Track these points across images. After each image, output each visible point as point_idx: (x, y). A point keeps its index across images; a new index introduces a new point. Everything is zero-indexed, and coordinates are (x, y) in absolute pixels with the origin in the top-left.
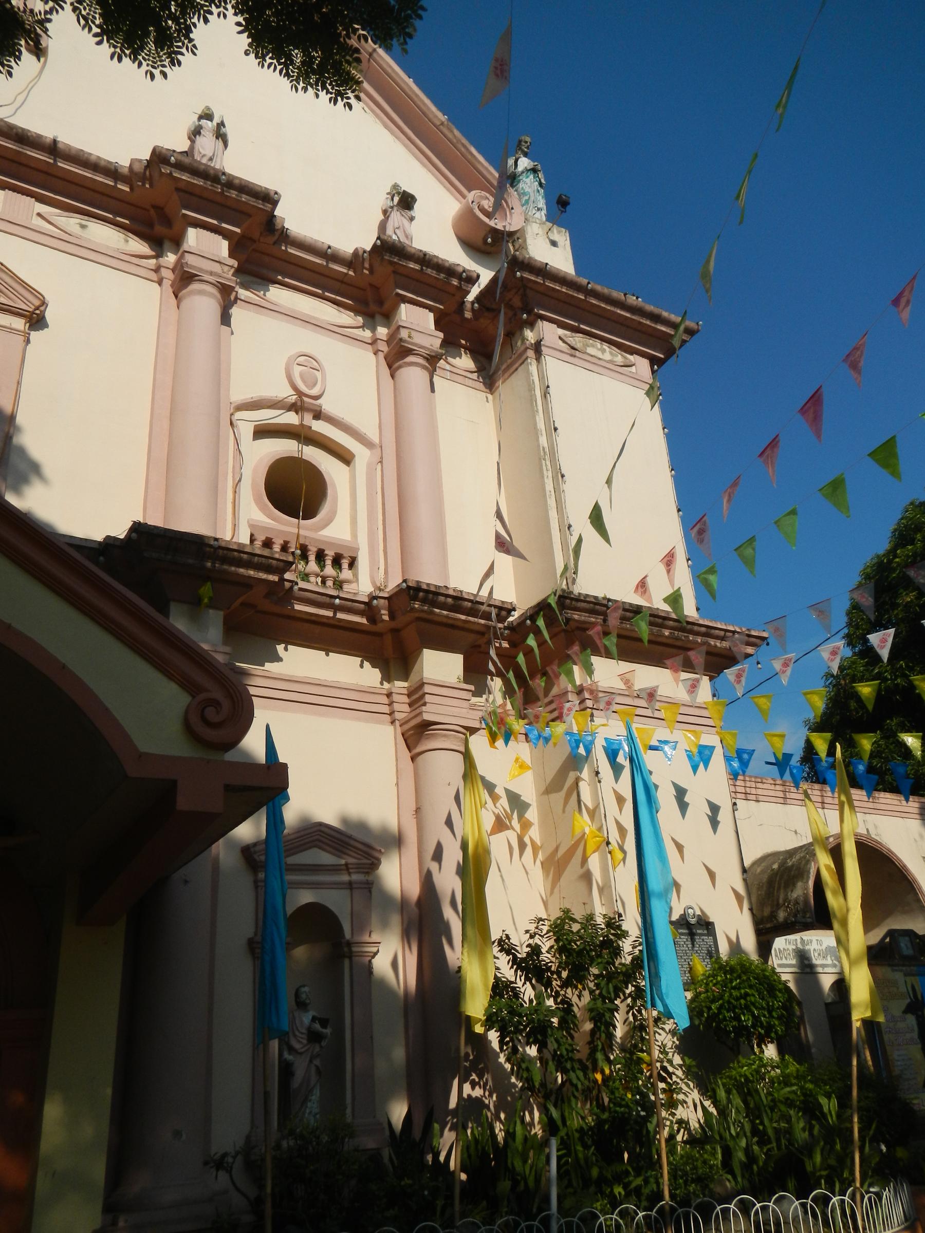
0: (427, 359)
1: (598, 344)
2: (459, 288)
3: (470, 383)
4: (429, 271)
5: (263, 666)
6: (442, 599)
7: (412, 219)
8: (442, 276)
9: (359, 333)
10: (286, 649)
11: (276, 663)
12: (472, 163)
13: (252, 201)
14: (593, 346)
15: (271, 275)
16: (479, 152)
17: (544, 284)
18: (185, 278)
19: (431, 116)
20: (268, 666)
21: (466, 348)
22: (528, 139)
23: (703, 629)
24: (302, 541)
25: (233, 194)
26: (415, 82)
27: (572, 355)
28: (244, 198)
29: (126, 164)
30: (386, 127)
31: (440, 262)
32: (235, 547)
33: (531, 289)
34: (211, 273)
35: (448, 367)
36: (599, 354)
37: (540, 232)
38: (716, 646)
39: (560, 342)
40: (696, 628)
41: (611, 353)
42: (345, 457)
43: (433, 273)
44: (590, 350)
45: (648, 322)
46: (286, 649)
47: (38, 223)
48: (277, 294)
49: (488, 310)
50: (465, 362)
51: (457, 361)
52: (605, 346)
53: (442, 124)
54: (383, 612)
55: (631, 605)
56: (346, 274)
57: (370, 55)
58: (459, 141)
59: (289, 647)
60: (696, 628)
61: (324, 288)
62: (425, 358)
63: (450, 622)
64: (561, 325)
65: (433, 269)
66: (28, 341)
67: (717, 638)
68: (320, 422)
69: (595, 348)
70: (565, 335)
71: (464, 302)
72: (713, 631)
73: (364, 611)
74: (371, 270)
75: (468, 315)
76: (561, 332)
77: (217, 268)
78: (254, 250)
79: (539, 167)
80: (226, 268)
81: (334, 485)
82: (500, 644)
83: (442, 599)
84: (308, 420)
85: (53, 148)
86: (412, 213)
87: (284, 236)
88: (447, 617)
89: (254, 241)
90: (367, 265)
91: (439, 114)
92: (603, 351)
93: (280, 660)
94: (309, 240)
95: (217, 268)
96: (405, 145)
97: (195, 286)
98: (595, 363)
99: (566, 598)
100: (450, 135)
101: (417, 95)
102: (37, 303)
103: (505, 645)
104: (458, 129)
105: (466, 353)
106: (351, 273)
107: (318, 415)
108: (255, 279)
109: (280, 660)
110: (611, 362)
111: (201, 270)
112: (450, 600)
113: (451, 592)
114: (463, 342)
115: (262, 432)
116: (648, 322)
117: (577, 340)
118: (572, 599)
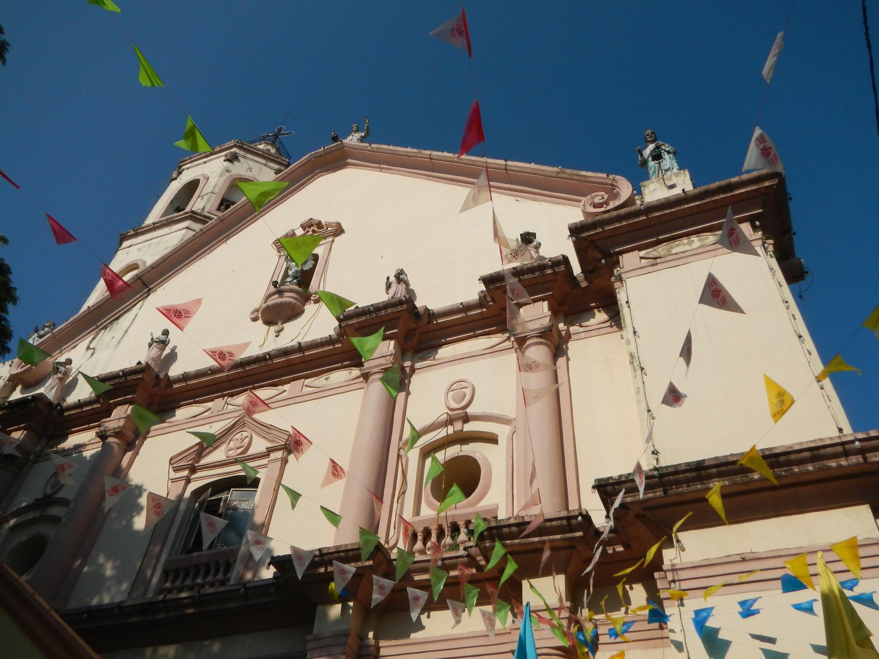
0: (541, 337)
1: (685, 240)
2: (554, 273)
3: (605, 331)
4: (526, 277)
5: (408, 636)
6: (506, 530)
7: (537, 247)
8: (537, 274)
9: (508, 344)
10: (428, 617)
11: (420, 632)
12: (585, 180)
13: (394, 310)
14: (678, 245)
15: (436, 342)
16: (587, 171)
17: (604, 230)
18: (366, 376)
19: (550, 174)
20: (414, 636)
21: (597, 307)
22: (649, 132)
23: (806, 454)
24: (450, 520)
25: (383, 312)
26: (536, 163)
27: (653, 265)
28: (389, 311)
29: (333, 333)
30: (533, 200)
31: (530, 266)
32: (333, 550)
33: (598, 240)
34: (376, 366)
35: (582, 329)
36: (687, 248)
37: (658, 185)
38: (840, 467)
39: (643, 261)
40: (793, 457)
41: (700, 240)
42: (492, 439)
43: (530, 276)
44: (674, 251)
45: (722, 196)
46: (428, 617)
47: (306, 390)
48: (444, 352)
49: (591, 272)
50: (601, 316)
51: (592, 321)
52: (694, 238)
53: (558, 173)
54: (478, 558)
55: (688, 464)
56: (482, 313)
57: (506, 169)
58: (571, 175)
59: (432, 613)
60: (793, 457)
61: (474, 329)
62: (537, 337)
63: (531, 547)
64: (640, 248)
65: (527, 273)
66: (286, 462)
67: (836, 456)
68: (471, 423)
69: (681, 246)
70: (647, 253)
71: (575, 278)
72: (822, 451)
73: (469, 562)
74: (493, 300)
75: (584, 284)
76: (642, 253)
77: (383, 361)
78: (421, 334)
79: (660, 143)
80: (388, 358)
81: (488, 465)
82: (614, 549)
83: (506, 530)
84: (458, 426)
85: (300, 348)
86: (534, 243)
87: (430, 315)
88: (519, 544)
89: (415, 329)
90: (489, 299)
91: (555, 169)
92: (690, 244)
93: (423, 628)
94: (447, 308)
95: (383, 361)
96: (548, 202)
97: (371, 378)
98: (684, 257)
99: (606, 485)
100: (565, 176)
101: (537, 170)
102: (286, 437)
103: (620, 549)
104: (568, 168)
105: (599, 311)
106: (484, 310)
107: (466, 419)
108: (425, 352)
109: (423, 628)
110: (700, 247)
111: (371, 368)
112: (514, 529)
113: (512, 521)
114: (593, 304)
115: (428, 452)
116: (722, 196)
117: (661, 250)
118: (613, 484)
